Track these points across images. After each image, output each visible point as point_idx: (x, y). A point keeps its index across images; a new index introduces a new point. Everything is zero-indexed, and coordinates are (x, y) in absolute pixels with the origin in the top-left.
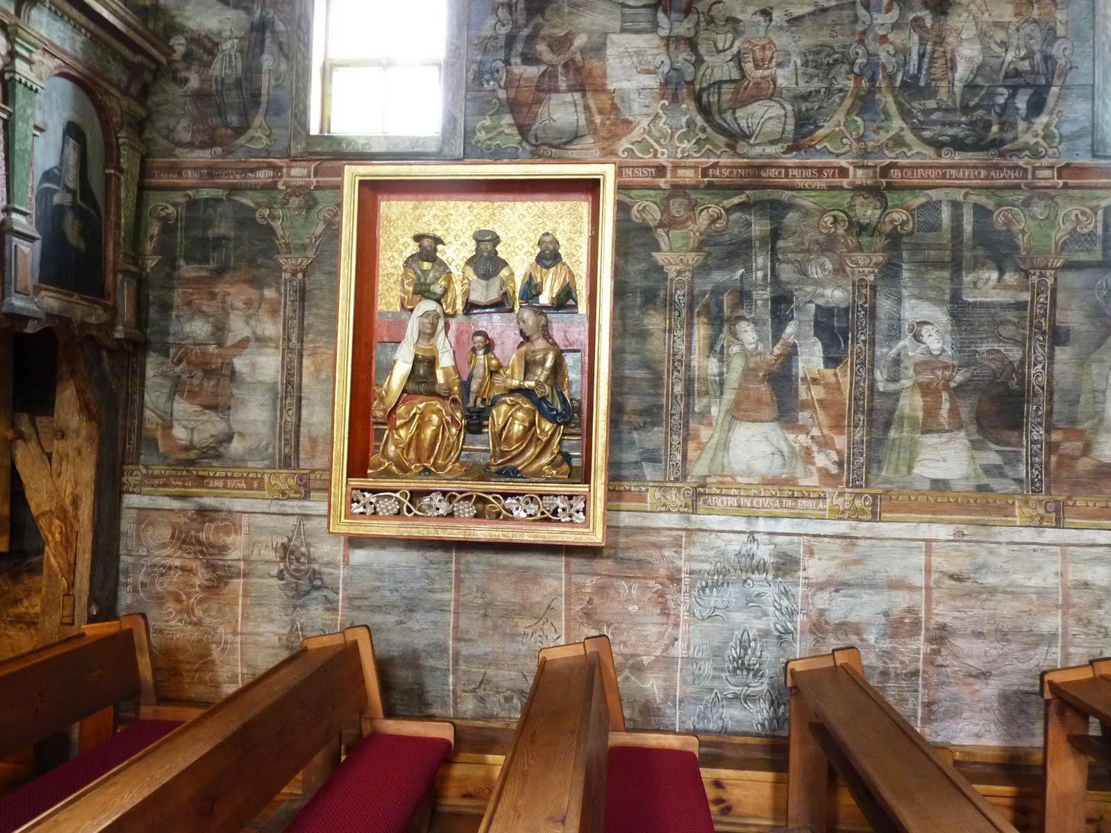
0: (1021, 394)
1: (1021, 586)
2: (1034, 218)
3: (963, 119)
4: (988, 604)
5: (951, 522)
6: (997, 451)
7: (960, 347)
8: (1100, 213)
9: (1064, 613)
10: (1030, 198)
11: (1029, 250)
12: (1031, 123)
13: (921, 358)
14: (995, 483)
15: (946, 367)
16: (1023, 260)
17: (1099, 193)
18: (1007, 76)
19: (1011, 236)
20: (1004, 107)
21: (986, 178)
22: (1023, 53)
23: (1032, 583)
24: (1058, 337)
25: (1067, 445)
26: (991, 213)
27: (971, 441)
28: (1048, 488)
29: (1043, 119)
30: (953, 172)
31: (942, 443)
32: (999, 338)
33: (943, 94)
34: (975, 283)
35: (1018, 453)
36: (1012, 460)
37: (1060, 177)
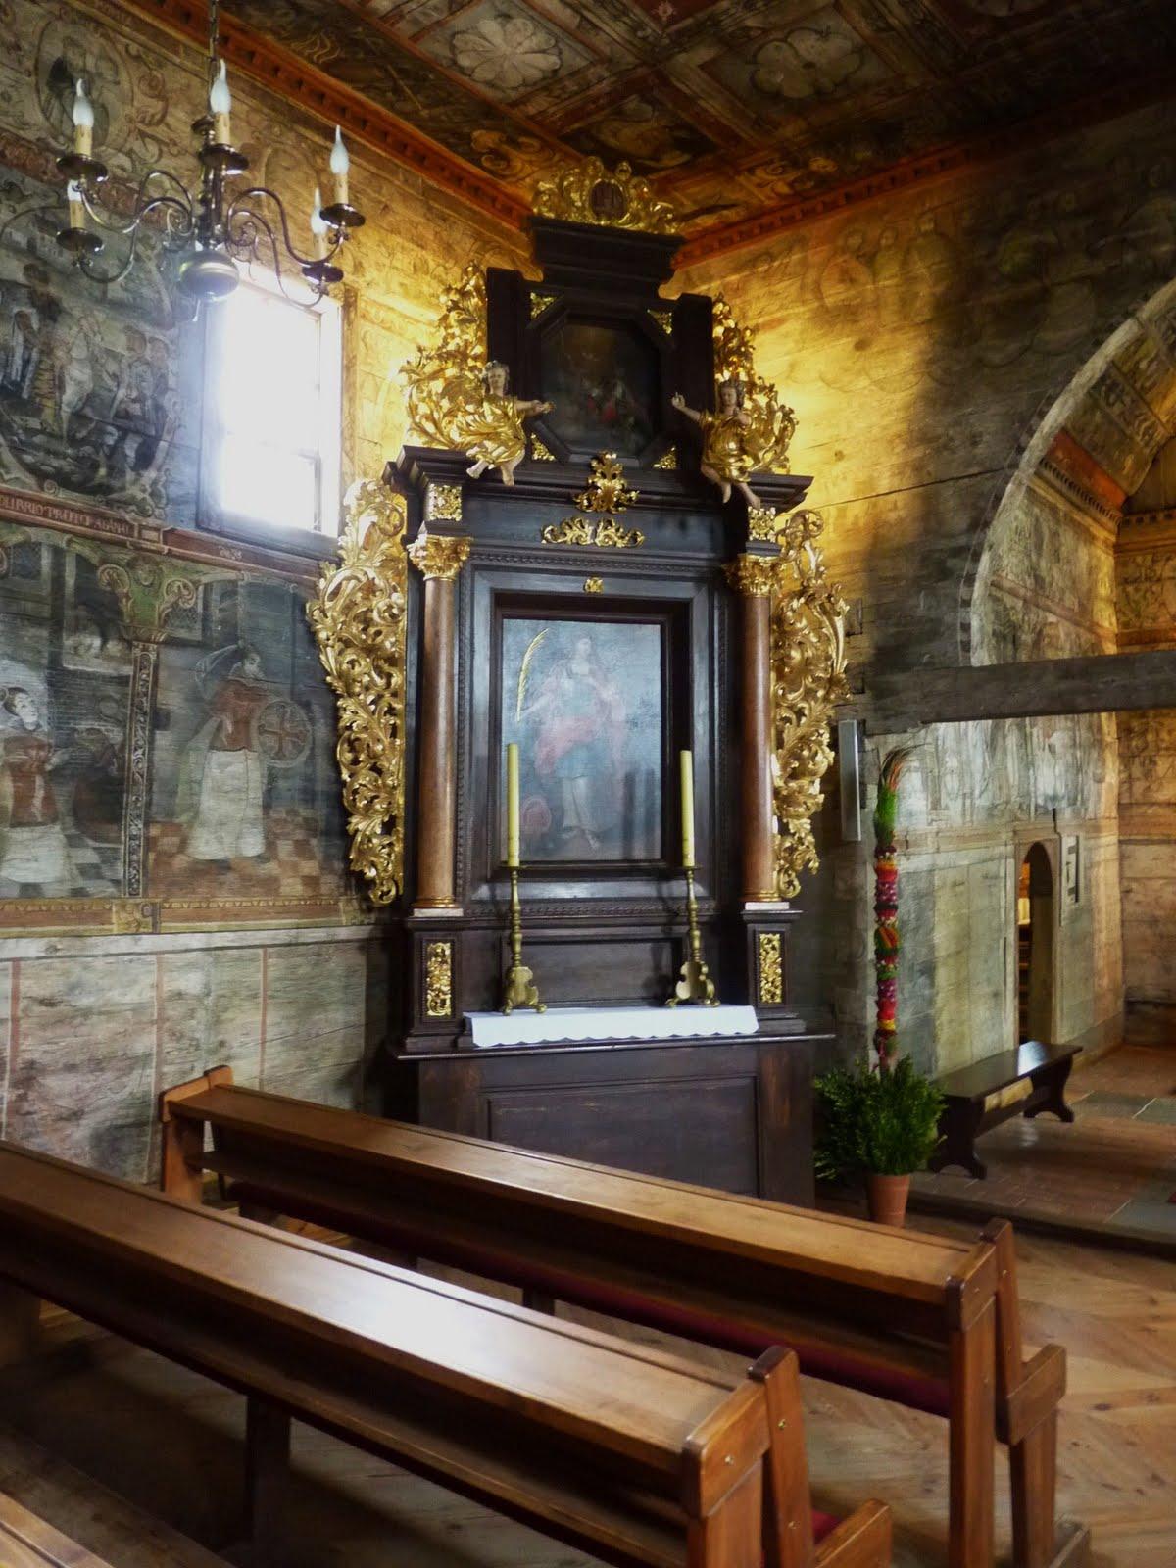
0: (121, 781)
1: (118, 1004)
2: (138, 582)
3: (69, 451)
4: (84, 1030)
5: (43, 935)
6: (95, 848)
7: (59, 722)
8: (201, 588)
9: (159, 1029)
10: (135, 559)
11: (133, 618)
12: (139, 476)
13: (14, 733)
14: (92, 886)
15: (41, 746)
16: (127, 628)
17: (201, 567)
18: (117, 415)
19: (115, 599)
20: (113, 449)
21: (90, 527)
22: (134, 394)
23: (128, 999)
24: (159, 720)
25: (165, 840)
26: (93, 568)
27: (67, 836)
28: (145, 890)
29: (150, 475)
30: (56, 511)
31: (34, 840)
32: (99, 716)
33: (48, 414)
34: (76, 648)
35: (116, 850)
36: (109, 858)
37: (165, 543)
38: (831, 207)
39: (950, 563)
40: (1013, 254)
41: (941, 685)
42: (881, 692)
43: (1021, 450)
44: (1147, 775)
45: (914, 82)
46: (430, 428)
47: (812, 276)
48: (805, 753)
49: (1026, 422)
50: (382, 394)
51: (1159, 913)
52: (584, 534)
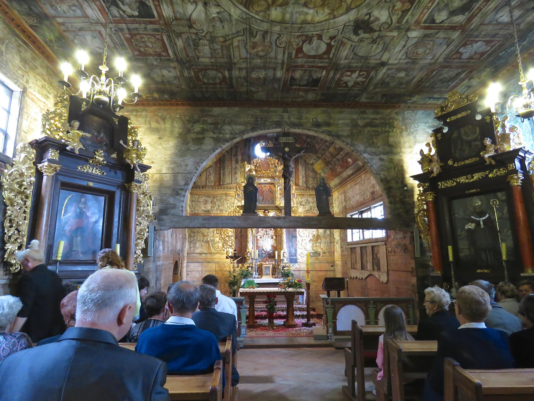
38: (155, 105)
39: (180, 192)
40: (198, 128)
41: (175, 220)
42: (160, 220)
43: (197, 170)
44: (194, 246)
45: (183, 87)
46: (49, 132)
47: (148, 119)
48: (142, 233)
49: (198, 164)
50: (29, 119)
51: (195, 280)
52: (87, 169)
